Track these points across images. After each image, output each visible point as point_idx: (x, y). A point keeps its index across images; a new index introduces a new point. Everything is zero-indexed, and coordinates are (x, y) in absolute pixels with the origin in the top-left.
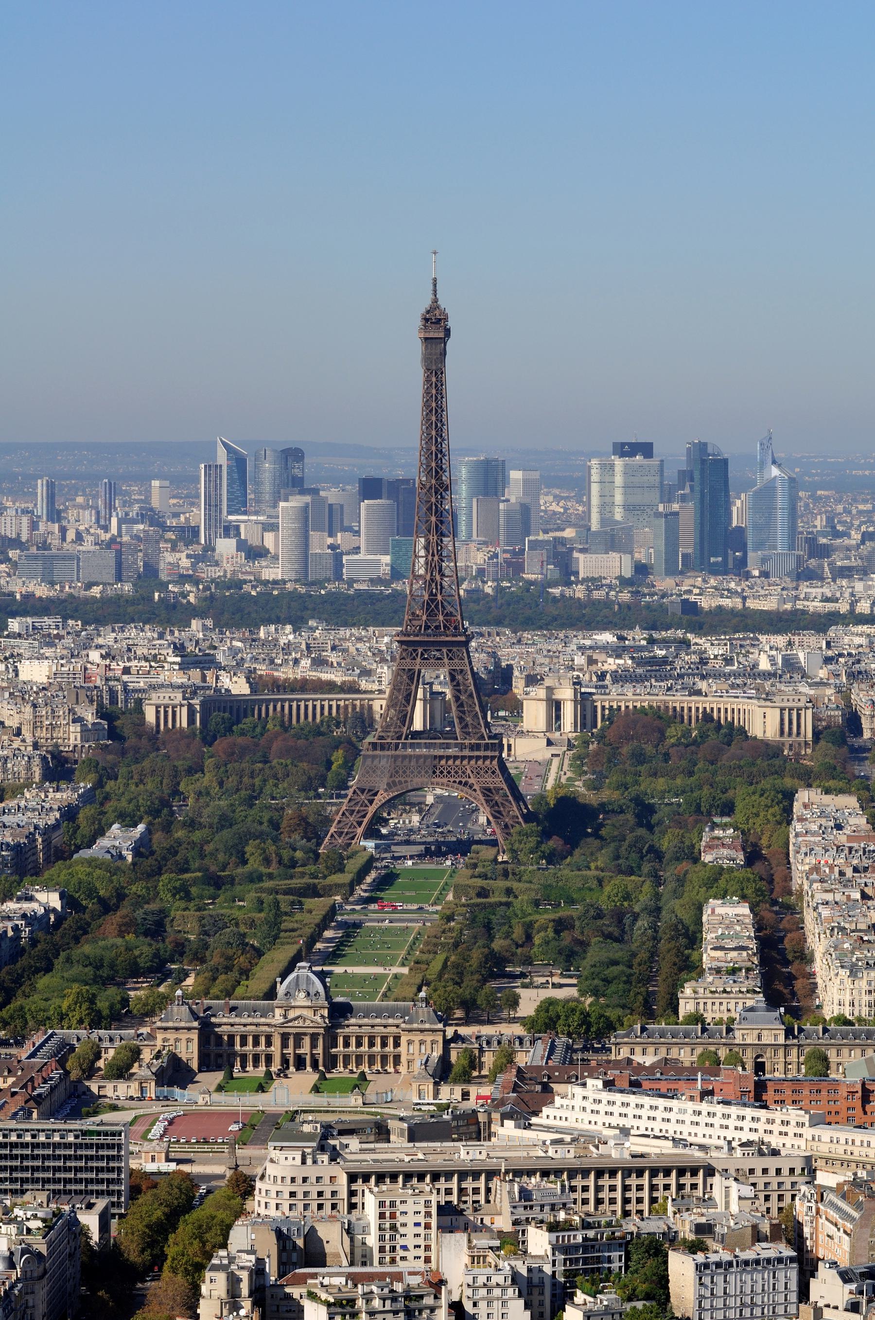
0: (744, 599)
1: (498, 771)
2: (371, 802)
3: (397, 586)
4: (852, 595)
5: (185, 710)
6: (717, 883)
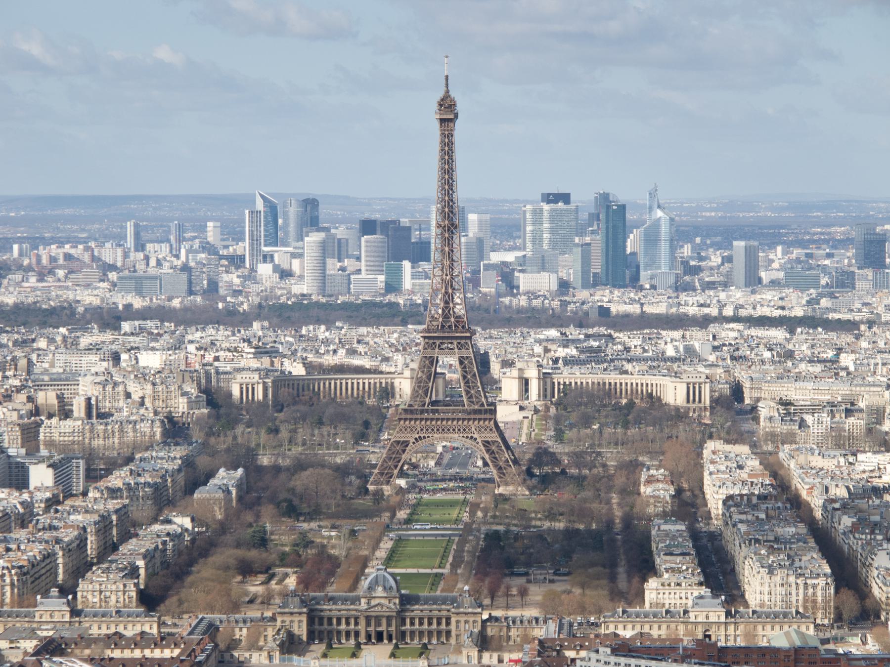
0: (642, 305)
1: (494, 429)
2: (404, 451)
3: (391, 298)
4: (719, 301)
5: (261, 386)
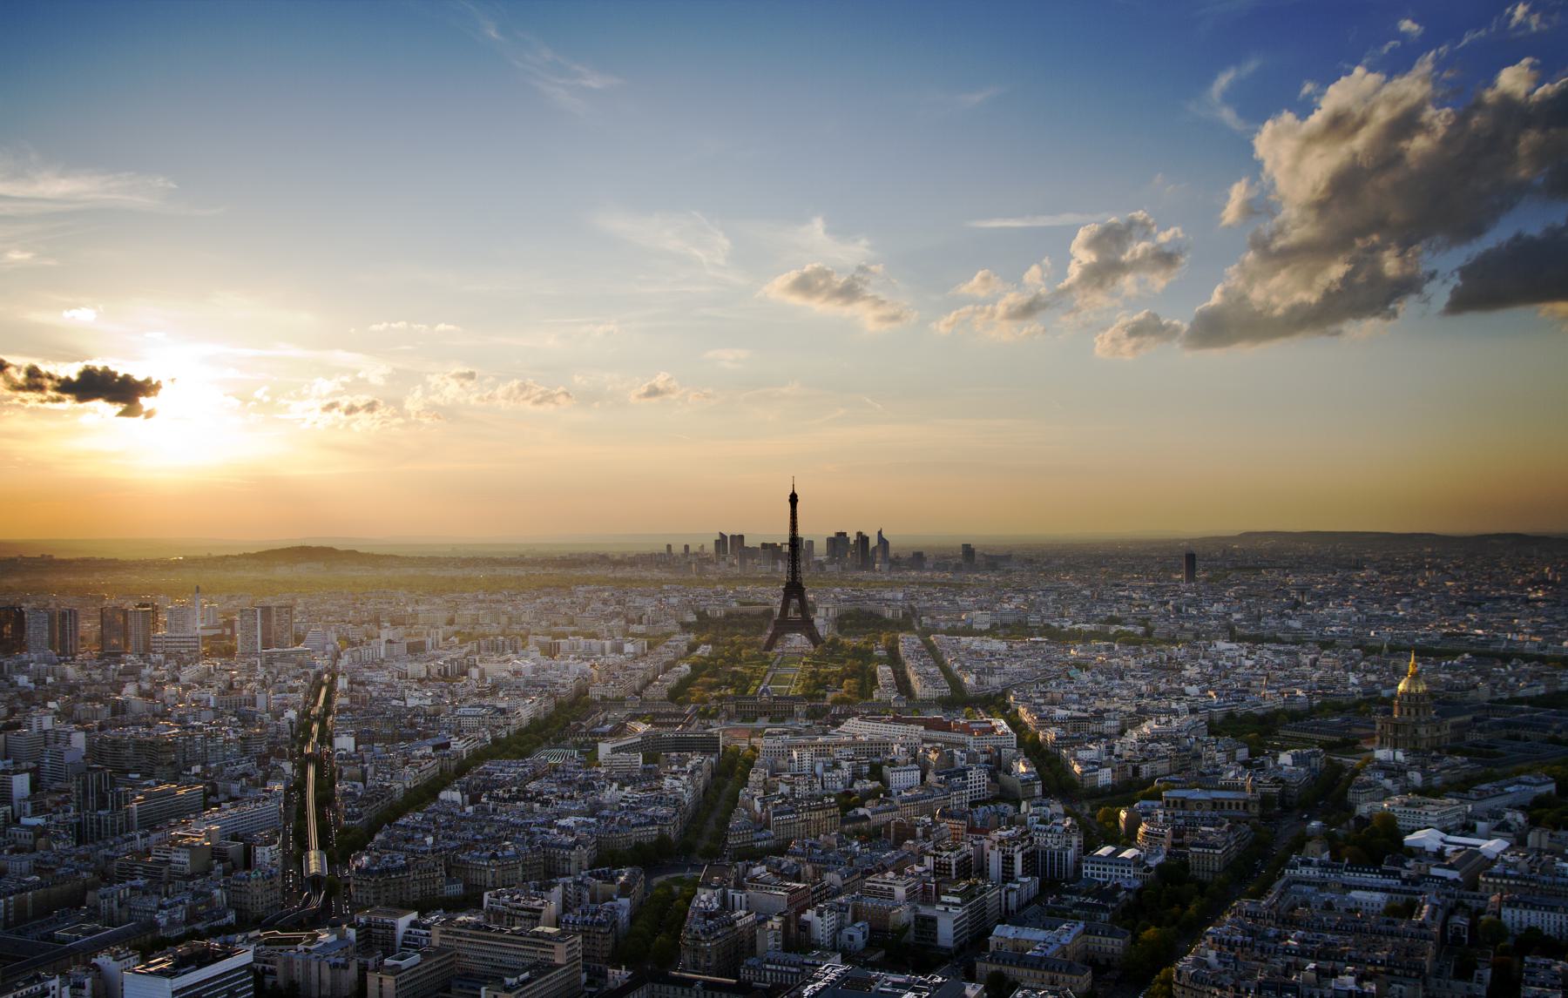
6: (881, 661)
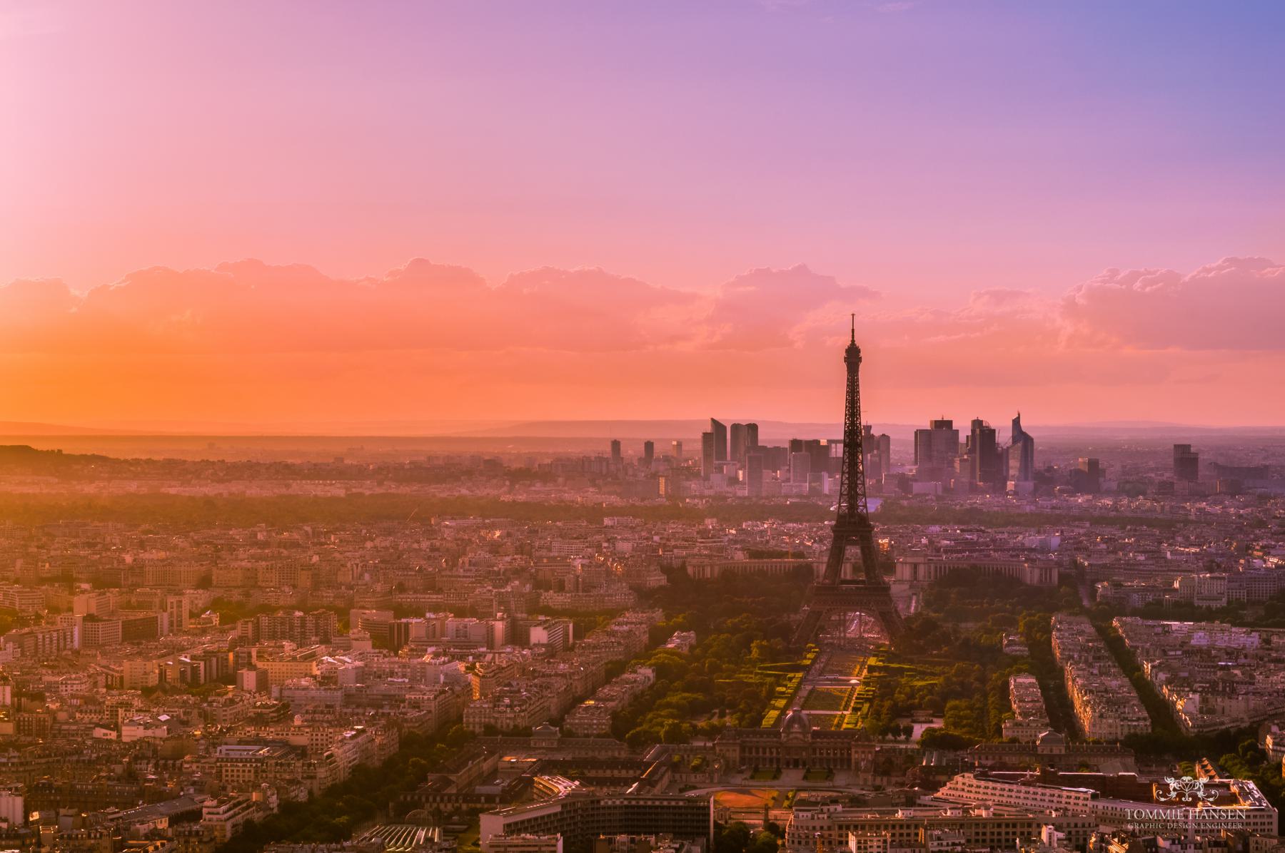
6: (1015, 664)
